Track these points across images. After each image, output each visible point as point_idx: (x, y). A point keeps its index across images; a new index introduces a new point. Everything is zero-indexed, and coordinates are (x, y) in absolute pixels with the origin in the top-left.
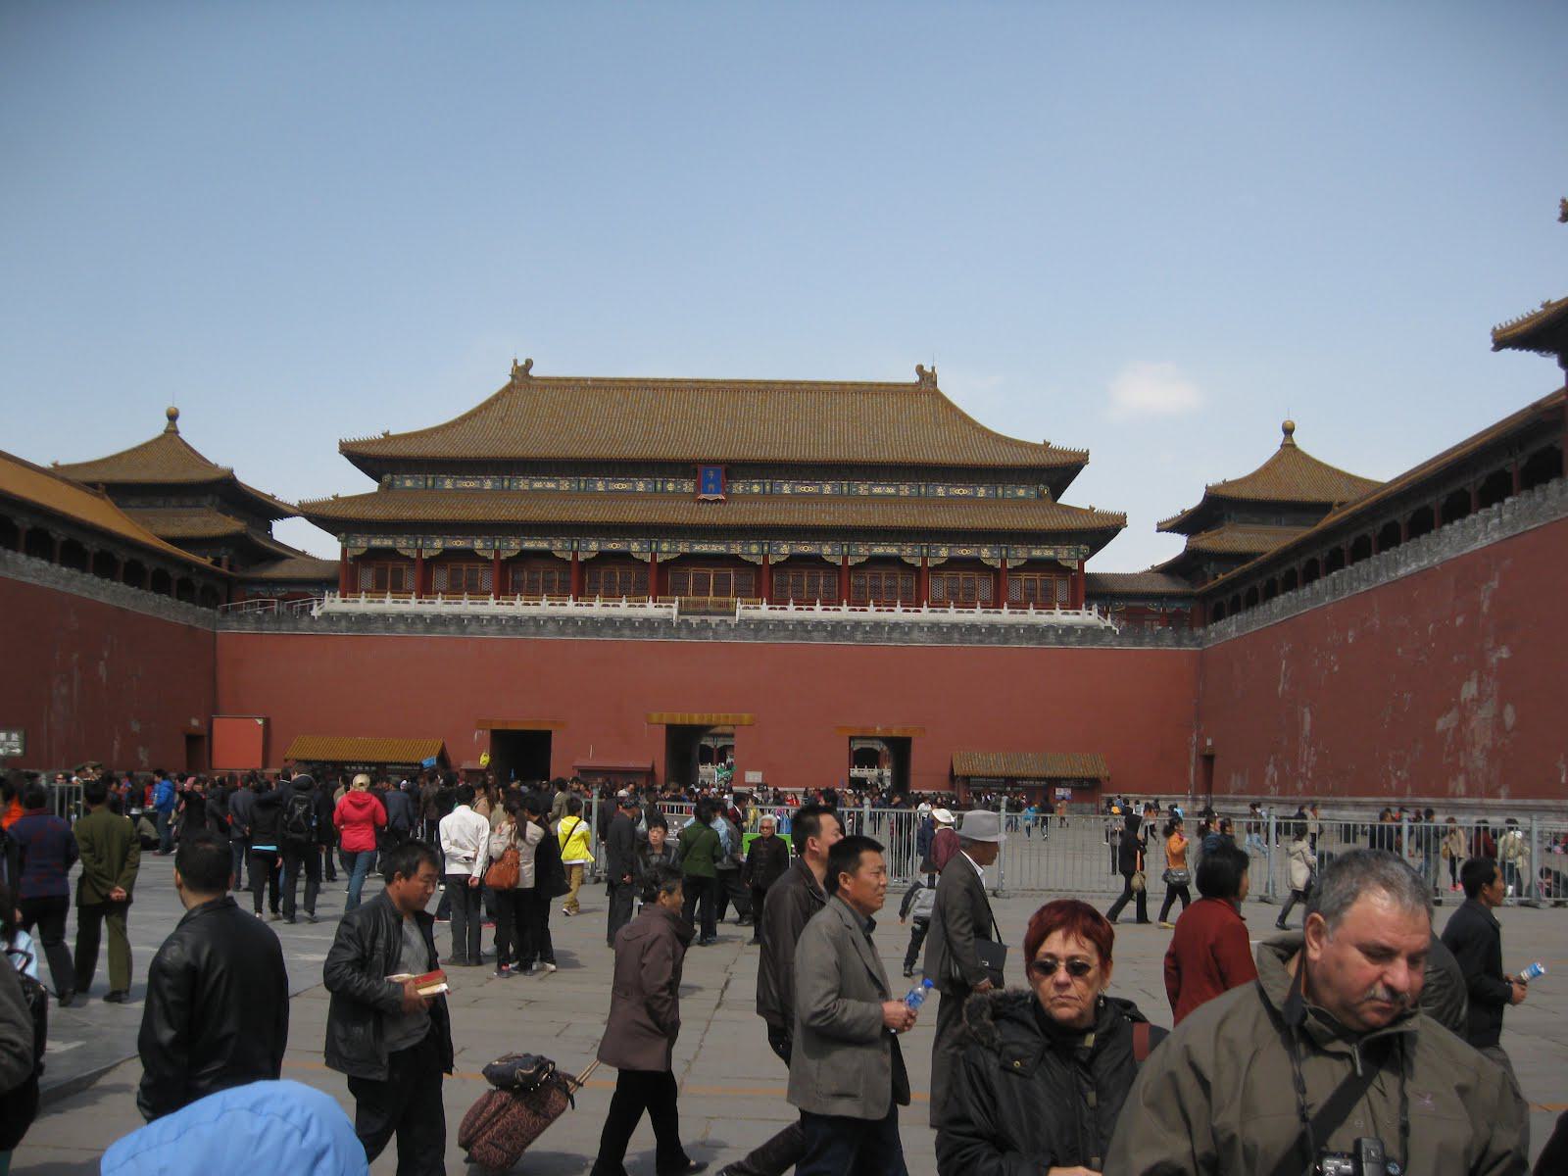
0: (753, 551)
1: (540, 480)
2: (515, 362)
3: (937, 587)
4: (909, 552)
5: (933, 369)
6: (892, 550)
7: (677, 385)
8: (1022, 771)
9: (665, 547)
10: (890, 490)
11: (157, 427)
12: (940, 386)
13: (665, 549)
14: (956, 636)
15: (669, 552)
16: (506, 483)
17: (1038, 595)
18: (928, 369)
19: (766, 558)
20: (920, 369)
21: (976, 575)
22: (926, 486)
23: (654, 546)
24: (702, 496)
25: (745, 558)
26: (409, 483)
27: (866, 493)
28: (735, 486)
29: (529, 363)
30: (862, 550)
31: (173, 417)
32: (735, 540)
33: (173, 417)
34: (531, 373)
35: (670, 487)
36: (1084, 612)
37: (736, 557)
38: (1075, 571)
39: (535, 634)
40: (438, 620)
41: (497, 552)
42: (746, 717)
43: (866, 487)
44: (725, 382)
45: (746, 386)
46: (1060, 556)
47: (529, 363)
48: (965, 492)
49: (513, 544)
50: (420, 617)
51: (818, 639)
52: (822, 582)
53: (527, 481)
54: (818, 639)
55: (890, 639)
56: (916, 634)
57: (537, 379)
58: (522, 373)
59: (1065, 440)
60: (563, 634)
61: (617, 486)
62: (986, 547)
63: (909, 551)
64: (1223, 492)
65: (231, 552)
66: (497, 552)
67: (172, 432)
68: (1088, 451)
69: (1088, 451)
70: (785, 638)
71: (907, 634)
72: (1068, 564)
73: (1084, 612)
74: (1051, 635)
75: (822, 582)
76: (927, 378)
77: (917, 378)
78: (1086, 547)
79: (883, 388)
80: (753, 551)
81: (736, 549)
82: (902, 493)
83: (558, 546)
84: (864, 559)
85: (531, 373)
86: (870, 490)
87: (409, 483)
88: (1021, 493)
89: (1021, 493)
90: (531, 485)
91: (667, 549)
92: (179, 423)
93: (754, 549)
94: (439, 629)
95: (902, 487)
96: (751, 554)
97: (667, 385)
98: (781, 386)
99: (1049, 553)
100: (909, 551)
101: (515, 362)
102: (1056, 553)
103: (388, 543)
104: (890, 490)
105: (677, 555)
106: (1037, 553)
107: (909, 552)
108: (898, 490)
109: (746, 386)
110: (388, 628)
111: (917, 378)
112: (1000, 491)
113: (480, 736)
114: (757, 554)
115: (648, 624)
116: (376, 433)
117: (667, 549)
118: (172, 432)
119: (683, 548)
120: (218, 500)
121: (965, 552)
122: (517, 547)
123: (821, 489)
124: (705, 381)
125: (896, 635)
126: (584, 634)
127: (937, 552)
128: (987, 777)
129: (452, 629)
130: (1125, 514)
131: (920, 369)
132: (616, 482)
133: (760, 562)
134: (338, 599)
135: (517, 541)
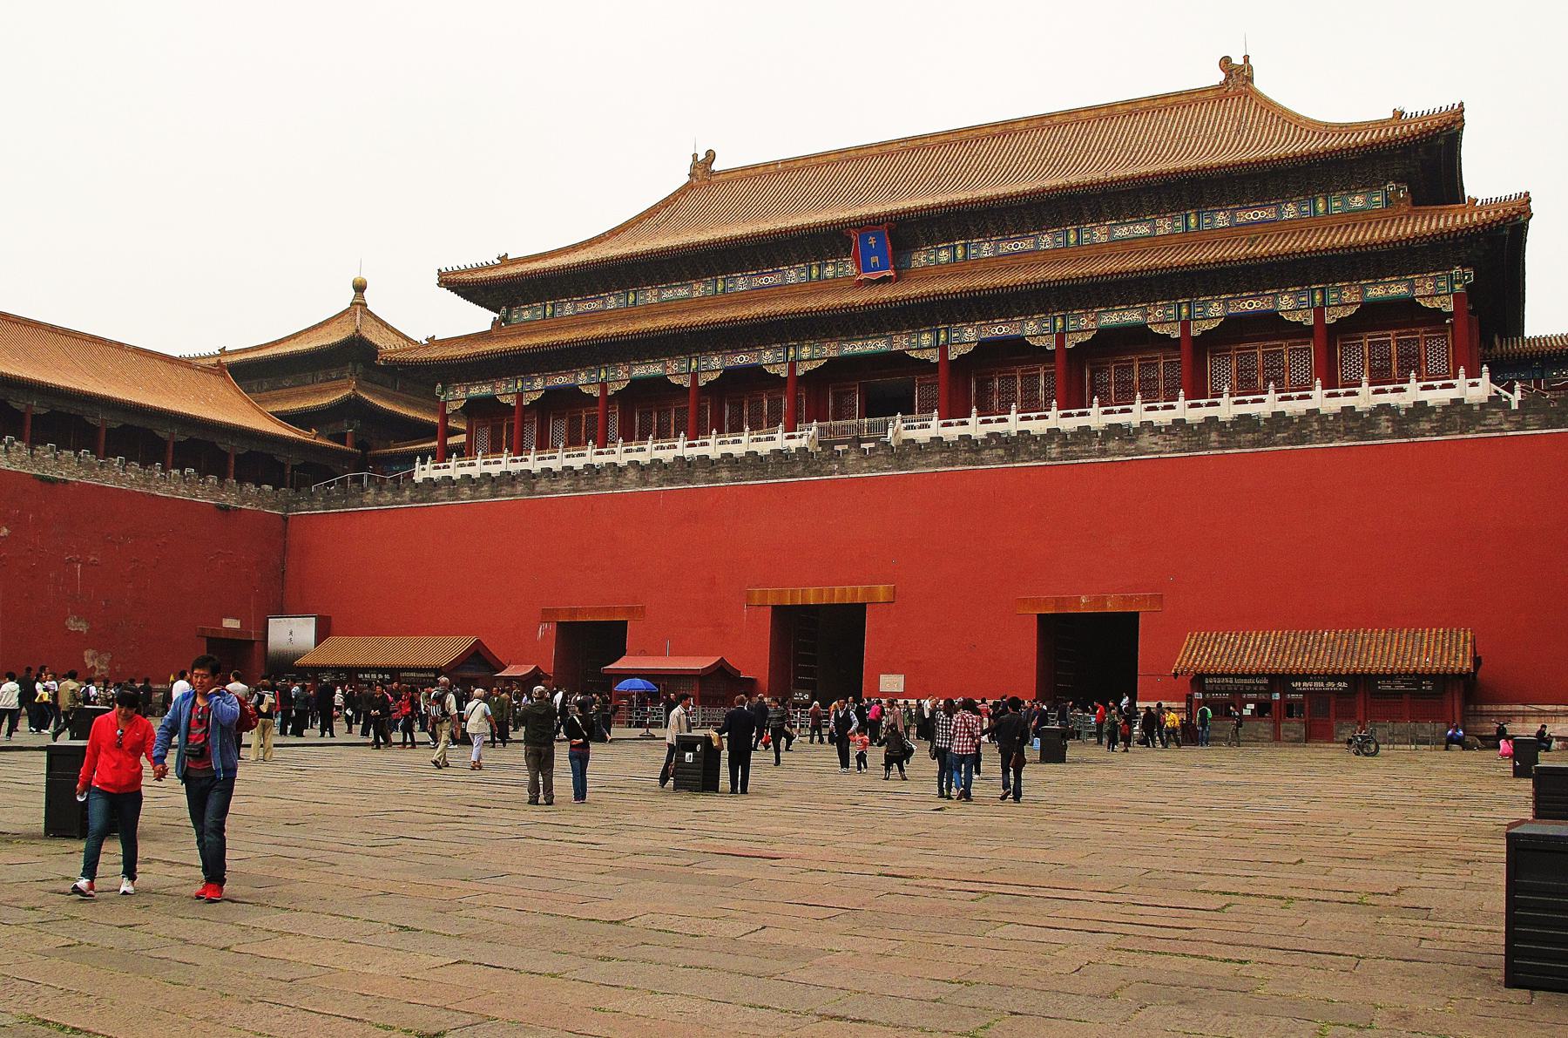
1: (668, 288)
2: (695, 156)
3: (1221, 369)
4: (1161, 318)
5: (1246, 58)
7: (888, 148)
8: (1300, 663)
9: (806, 352)
10: (1142, 230)
11: (346, 298)
13: (805, 356)
14: (1214, 436)
15: (809, 359)
16: (631, 298)
17: (1394, 367)
18: (1238, 60)
19: (944, 350)
20: (1225, 62)
21: (1285, 346)
22: (1197, 214)
23: (791, 353)
24: (863, 276)
25: (913, 354)
26: (527, 315)
27: (1104, 239)
28: (915, 256)
29: (711, 155)
30: (1084, 322)
31: (360, 288)
32: (898, 329)
33: (360, 288)
34: (716, 167)
35: (829, 271)
36: (1462, 381)
37: (901, 355)
38: (1450, 315)
39: (612, 487)
40: (508, 479)
41: (603, 386)
42: (882, 591)
43: (1104, 229)
44: (949, 133)
45: (976, 133)
46: (1419, 292)
47: (711, 155)
48: (1261, 214)
49: (622, 373)
50: (486, 476)
51: (992, 463)
52: (1042, 382)
53: (655, 292)
54: (992, 463)
55: (1104, 452)
56: (1146, 440)
57: (719, 173)
58: (703, 168)
59: (1422, 99)
60: (645, 485)
61: (762, 281)
62: (1286, 293)
63: (1158, 314)
65: (357, 423)
66: (603, 386)
67: (359, 305)
68: (1461, 105)
69: (1461, 105)
70: (942, 463)
71: (1132, 441)
72: (1437, 303)
73: (1462, 381)
74: (1384, 424)
75: (1042, 382)
76: (1237, 75)
77: (1220, 77)
78: (1467, 271)
79: (1170, 100)
80: (921, 344)
81: (901, 343)
82: (1160, 232)
83: (675, 371)
84: (1088, 336)
85: (716, 167)
86: (1110, 233)
87: (527, 315)
88: (1358, 201)
90: (659, 295)
91: (811, 356)
92: (368, 295)
93: (926, 339)
94: (506, 489)
95: (1159, 222)
96: (921, 349)
97: (875, 151)
98: (1022, 125)
99: (1398, 290)
100: (1158, 314)
101: (695, 156)
102: (1412, 287)
104: (1142, 230)
105: (821, 363)
106: (1376, 293)
107: (1161, 318)
108: (1154, 228)
109: (976, 133)
110: (454, 495)
111: (1221, 76)
112: (1321, 206)
113: (545, 632)
114: (930, 347)
115: (754, 462)
116: (492, 258)
118: (359, 305)
119: (830, 350)
120: (360, 367)
121: (1251, 305)
122: (626, 376)
123: (1036, 244)
124: (922, 137)
125: (1111, 445)
126: (671, 481)
127: (1205, 310)
128: (1236, 676)
129: (520, 488)
130: (1527, 194)
131: (1225, 62)
132: (760, 275)
133: (933, 356)
135: (626, 368)
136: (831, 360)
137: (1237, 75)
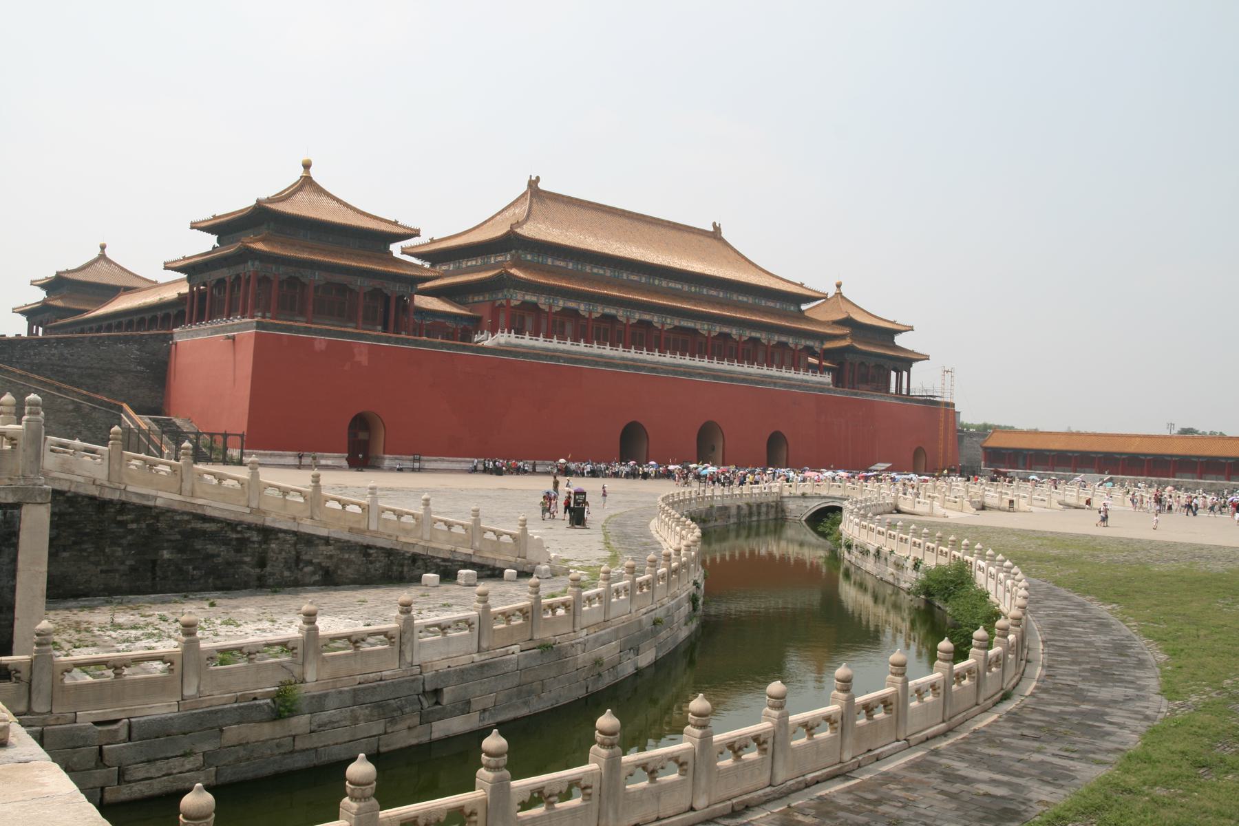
11: (300, 171)
12: (723, 235)
20: (714, 224)
29: (538, 178)
33: (307, 166)
35: (657, 282)
47: (538, 178)
76: (717, 229)
77: (711, 229)
81: (698, 326)
87: (529, 257)
91: (671, 322)
93: (706, 327)
103: (534, 299)
111: (711, 229)
117: (671, 322)
119: (676, 323)
131: (714, 224)
134: (513, 334)
136: (676, 327)
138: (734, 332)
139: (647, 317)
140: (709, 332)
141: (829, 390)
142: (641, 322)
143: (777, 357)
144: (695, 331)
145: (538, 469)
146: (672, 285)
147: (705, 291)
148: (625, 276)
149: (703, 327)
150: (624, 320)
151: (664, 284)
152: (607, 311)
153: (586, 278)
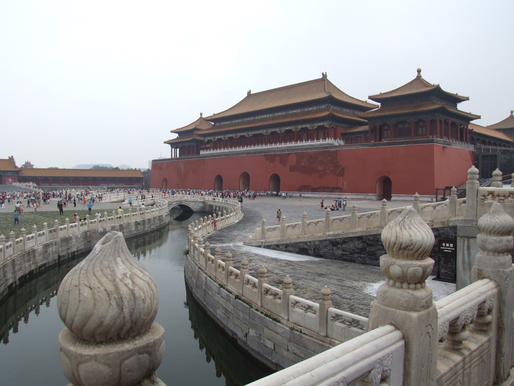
0: (263, 132)
6: (289, 128)
10: (296, 111)
12: (328, 78)
20: (323, 74)
34: (251, 93)
35: (256, 118)
58: (249, 93)
64: (394, 95)
76: (325, 76)
77: (321, 77)
81: (261, 132)
85: (251, 93)
88: (323, 107)
89: (323, 107)
91: (251, 133)
116: (211, 114)
119: (253, 133)
131: (323, 74)
137: (325, 76)
138: (277, 130)
139: (304, 126)
140: (267, 133)
141: (343, 146)
142: (241, 136)
143: (315, 135)
144: (261, 135)
145: (303, 195)
146: (262, 117)
147: (276, 115)
148: (306, 110)
149: (263, 132)
150: (279, 132)
151: (259, 117)
152: (287, 128)
153: (235, 125)
